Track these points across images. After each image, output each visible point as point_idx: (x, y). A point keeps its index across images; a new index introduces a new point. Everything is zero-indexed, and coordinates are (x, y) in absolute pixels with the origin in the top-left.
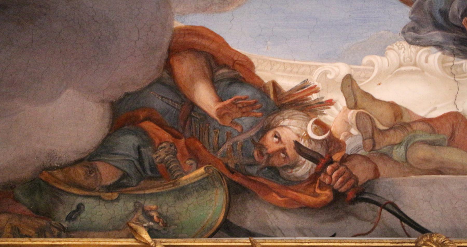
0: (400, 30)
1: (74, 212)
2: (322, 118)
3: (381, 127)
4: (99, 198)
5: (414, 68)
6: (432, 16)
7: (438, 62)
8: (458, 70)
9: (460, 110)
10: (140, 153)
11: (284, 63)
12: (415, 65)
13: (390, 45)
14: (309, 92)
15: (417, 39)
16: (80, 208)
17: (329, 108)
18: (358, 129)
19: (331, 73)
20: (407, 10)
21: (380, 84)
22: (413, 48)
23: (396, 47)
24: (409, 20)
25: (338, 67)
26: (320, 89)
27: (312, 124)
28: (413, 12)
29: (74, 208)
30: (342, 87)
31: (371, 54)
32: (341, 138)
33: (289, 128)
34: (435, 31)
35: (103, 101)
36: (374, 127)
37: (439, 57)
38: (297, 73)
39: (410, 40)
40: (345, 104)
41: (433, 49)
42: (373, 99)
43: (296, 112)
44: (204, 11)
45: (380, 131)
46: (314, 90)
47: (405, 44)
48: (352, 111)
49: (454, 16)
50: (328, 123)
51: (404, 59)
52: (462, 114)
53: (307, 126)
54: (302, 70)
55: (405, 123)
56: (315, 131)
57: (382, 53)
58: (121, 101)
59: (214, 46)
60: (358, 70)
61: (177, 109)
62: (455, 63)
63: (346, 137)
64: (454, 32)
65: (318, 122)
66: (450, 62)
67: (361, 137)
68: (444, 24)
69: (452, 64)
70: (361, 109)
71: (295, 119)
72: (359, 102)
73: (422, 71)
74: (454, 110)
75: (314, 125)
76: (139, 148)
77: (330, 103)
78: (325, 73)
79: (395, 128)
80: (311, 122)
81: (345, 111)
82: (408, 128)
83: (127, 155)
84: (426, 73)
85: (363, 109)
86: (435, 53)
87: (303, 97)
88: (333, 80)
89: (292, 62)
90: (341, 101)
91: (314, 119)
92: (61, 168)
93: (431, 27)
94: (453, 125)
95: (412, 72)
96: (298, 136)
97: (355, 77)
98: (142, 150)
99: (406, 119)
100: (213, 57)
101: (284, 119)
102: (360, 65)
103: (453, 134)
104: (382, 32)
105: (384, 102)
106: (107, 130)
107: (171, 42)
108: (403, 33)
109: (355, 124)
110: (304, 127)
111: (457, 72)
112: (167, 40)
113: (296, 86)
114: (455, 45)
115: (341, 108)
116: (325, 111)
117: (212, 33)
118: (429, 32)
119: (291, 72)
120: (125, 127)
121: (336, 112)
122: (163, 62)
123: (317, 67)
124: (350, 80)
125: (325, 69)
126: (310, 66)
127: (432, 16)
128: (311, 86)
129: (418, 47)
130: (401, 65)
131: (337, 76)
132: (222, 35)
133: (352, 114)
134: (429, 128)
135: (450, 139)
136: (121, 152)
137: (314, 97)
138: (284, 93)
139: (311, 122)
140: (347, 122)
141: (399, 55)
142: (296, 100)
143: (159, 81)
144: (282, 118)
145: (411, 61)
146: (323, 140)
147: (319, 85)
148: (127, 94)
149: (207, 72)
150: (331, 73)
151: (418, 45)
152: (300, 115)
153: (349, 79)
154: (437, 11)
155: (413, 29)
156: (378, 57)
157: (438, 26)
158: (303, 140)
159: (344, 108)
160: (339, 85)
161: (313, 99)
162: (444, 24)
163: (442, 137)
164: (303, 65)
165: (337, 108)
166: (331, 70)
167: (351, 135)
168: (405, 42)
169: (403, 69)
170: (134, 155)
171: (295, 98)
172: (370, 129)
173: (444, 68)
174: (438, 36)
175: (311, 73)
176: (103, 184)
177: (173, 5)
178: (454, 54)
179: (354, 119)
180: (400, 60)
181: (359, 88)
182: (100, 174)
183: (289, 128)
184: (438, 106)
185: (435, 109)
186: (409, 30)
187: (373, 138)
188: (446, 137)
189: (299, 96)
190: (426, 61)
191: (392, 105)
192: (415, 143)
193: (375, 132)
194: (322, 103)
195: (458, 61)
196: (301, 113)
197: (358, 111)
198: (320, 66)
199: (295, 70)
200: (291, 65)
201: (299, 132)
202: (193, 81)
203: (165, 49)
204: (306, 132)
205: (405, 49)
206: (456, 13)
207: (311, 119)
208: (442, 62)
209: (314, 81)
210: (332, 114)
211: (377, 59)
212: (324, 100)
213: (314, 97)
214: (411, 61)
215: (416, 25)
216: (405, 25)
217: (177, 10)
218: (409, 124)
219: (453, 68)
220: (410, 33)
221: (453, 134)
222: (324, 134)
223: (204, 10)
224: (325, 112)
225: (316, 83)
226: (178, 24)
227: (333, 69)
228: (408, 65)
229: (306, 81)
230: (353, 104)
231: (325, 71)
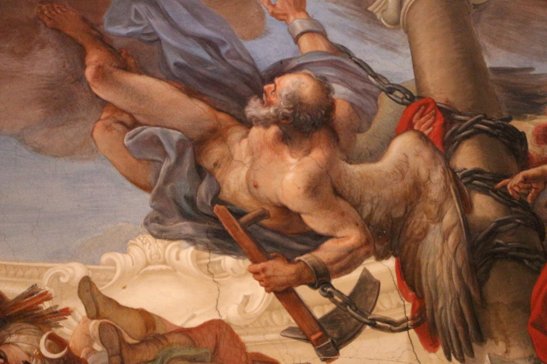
0: (142, 221)
2: (57, 332)
3: (130, 340)
5: (164, 267)
6: (177, 204)
7: (192, 258)
8: (217, 268)
9: (224, 318)
11: (5, 266)
12: (165, 263)
13: (132, 239)
14: (39, 300)
15: (162, 231)
17: (66, 319)
18: (103, 344)
19: (64, 276)
20: (147, 197)
21: (124, 288)
22: (160, 243)
23: (139, 242)
24: (150, 209)
25: (72, 268)
26: (53, 296)
27: (46, 340)
28: (154, 199)
30: (79, 292)
31: (111, 251)
32: (82, 356)
33: (17, 346)
34: (183, 221)
36: (122, 341)
37: (192, 252)
38: (23, 277)
39: (155, 232)
40: (84, 314)
41: (184, 243)
42: (118, 306)
43: (25, 326)
45: (129, 345)
46: (45, 297)
47: (150, 238)
48: (94, 322)
49: (202, 203)
50: (65, 338)
51: (151, 256)
52: (226, 322)
53: (39, 343)
54: (28, 273)
55: (159, 335)
56: (49, 348)
57: (124, 250)
60: (97, 271)
62: (213, 260)
63: (88, 354)
64: (205, 223)
65: (53, 337)
66: (205, 259)
67: (106, 354)
68: (193, 213)
69: (208, 261)
70: (105, 318)
71: (24, 334)
72: (102, 310)
73: (173, 271)
74: (216, 317)
75: (48, 341)
77: (66, 312)
78: (57, 276)
79: (147, 341)
80: (45, 337)
81: (85, 322)
82: (164, 341)
84: (178, 272)
85: (107, 318)
86: (187, 248)
87: (32, 306)
88: (67, 283)
89: (15, 264)
90: (80, 310)
91: (48, 333)
93: (177, 217)
94: (217, 336)
95: (161, 272)
96: (29, 355)
97: (93, 280)
99: (160, 330)
101: (10, 335)
102: (99, 264)
103: (216, 347)
104: (120, 224)
105: (132, 309)
108: (146, 224)
109: (98, 337)
110: (35, 344)
111: (215, 271)
113: (23, 294)
114: (208, 238)
115: (80, 318)
116: (61, 323)
118: (176, 223)
119: (15, 275)
121: (75, 324)
123: (47, 268)
124: (88, 285)
125: (57, 271)
126: (38, 268)
127: (177, 204)
128: (41, 292)
129: (166, 242)
130: (148, 264)
131: (72, 278)
133: (94, 325)
134: (188, 340)
135: (214, 353)
137: (46, 305)
138: (8, 302)
139: (45, 337)
140: (88, 336)
141: (144, 251)
142: (25, 310)
144: (6, 333)
145: (160, 258)
146: (59, 359)
147: (51, 291)
150: (64, 276)
151: (165, 238)
152: (32, 328)
153: (86, 281)
154: (182, 198)
155: (157, 220)
156: (119, 255)
157: (186, 216)
158: (34, 361)
159: (83, 317)
160: (76, 290)
161: (44, 309)
162: (193, 213)
163: (204, 351)
164: (29, 267)
165: (75, 318)
166: (64, 272)
167: (93, 351)
168: (150, 235)
169: (150, 268)
171: (23, 307)
172: (116, 343)
173: (199, 266)
174: (187, 228)
175: (40, 277)
178: (209, 249)
179: (96, 333)
180: (146, 256)
181: (100, 293)
183: (17, 346)
184: (197, 313)
185: (194, 316)
186: (152, 221)
187: (120, 354)
188: (208, 351)
189: (28, 305)
190: (178, 258)
191: (142, 312)
192: (172, 359)
193: (123, 346)
194: (57, 312)
195: (215, 257)
196: (32, 326)
197: (101, 321)
198: (50, 267)
199: (20, 273)
200: (14, 267)
201: (29, 350)
204: (39, 350)
205: (150, 244)
206: (205, 200)
207: (44, 333)
208: (197, 259)
209: (44, 285)
210: (69, 326)
211: (118, 257)
212: (58, 309)
213: (46, 305)
214: (160, 258)
215: (159, 215)
216: (146, 215)
218: (164, 336)
219: (210, 266)
220: (154, 224)
221: (216, 347)
222: (61, 351)
224: (61, 324)
225: (47, 289)
227: (66, 271)
228: (155, 264)
229: (34, 287)
230: (95, 313)
231: (57, 273)
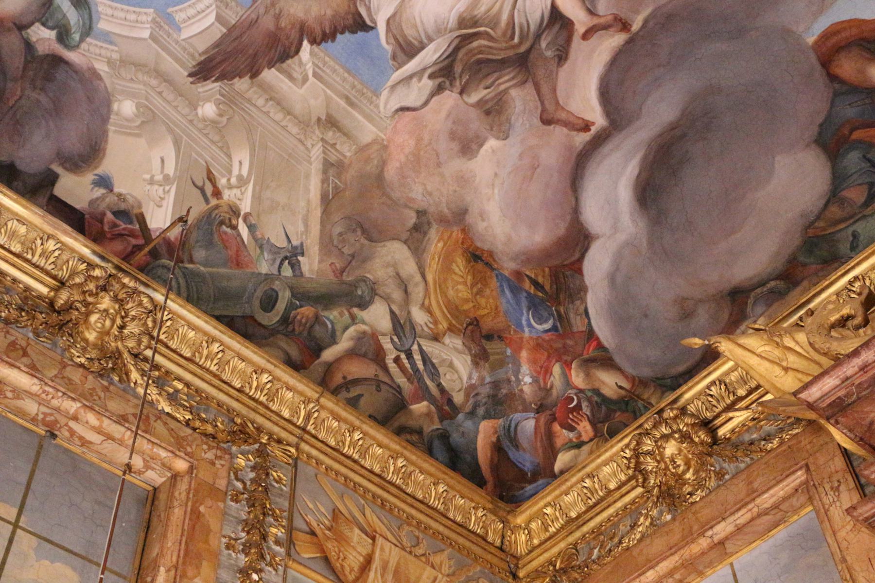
1: (852, 242)
4: (864, 217)
10: (869, 160)
16: (855, 235)
29: (851, 238)
35: (808, 146)
44: (822, 12)
58: (820, 134)
59: (854, 31)
61: (870, 104)
76: (864, 157)
83: (861, 169)
92: (818, 217)
98: (869, 156)
100: (863, 39)
106: (829, 164)
107: (818, 57)
112: (813, 58)
117: (843, 22)
120: (841, 150)
122: (826, 78)
132: (853, 17)
136: (854, 171)
143: (836, 94)
148: (821, 125)
149: (867, 56)
170: (865, 165)
176: (859, 204)
177: (795, 29)
182: (851, 199)
202: (862, 72)
203: (818, 67)
217: (801, 28)
223: (821, 11)
226: (811, 40)
